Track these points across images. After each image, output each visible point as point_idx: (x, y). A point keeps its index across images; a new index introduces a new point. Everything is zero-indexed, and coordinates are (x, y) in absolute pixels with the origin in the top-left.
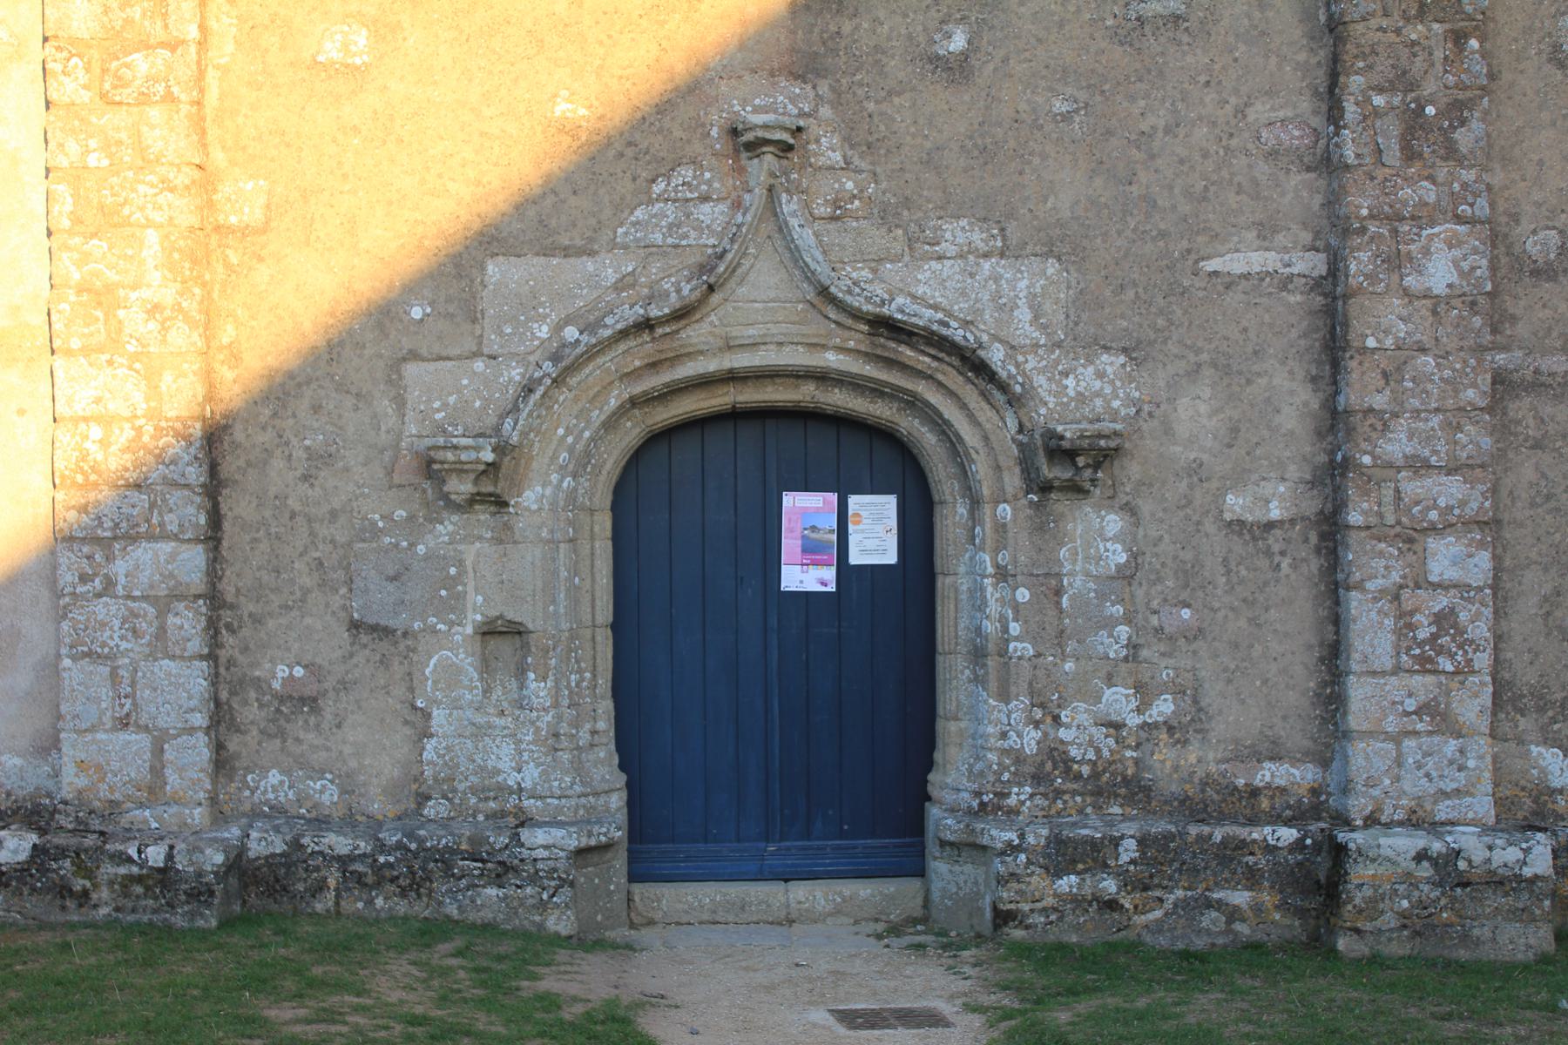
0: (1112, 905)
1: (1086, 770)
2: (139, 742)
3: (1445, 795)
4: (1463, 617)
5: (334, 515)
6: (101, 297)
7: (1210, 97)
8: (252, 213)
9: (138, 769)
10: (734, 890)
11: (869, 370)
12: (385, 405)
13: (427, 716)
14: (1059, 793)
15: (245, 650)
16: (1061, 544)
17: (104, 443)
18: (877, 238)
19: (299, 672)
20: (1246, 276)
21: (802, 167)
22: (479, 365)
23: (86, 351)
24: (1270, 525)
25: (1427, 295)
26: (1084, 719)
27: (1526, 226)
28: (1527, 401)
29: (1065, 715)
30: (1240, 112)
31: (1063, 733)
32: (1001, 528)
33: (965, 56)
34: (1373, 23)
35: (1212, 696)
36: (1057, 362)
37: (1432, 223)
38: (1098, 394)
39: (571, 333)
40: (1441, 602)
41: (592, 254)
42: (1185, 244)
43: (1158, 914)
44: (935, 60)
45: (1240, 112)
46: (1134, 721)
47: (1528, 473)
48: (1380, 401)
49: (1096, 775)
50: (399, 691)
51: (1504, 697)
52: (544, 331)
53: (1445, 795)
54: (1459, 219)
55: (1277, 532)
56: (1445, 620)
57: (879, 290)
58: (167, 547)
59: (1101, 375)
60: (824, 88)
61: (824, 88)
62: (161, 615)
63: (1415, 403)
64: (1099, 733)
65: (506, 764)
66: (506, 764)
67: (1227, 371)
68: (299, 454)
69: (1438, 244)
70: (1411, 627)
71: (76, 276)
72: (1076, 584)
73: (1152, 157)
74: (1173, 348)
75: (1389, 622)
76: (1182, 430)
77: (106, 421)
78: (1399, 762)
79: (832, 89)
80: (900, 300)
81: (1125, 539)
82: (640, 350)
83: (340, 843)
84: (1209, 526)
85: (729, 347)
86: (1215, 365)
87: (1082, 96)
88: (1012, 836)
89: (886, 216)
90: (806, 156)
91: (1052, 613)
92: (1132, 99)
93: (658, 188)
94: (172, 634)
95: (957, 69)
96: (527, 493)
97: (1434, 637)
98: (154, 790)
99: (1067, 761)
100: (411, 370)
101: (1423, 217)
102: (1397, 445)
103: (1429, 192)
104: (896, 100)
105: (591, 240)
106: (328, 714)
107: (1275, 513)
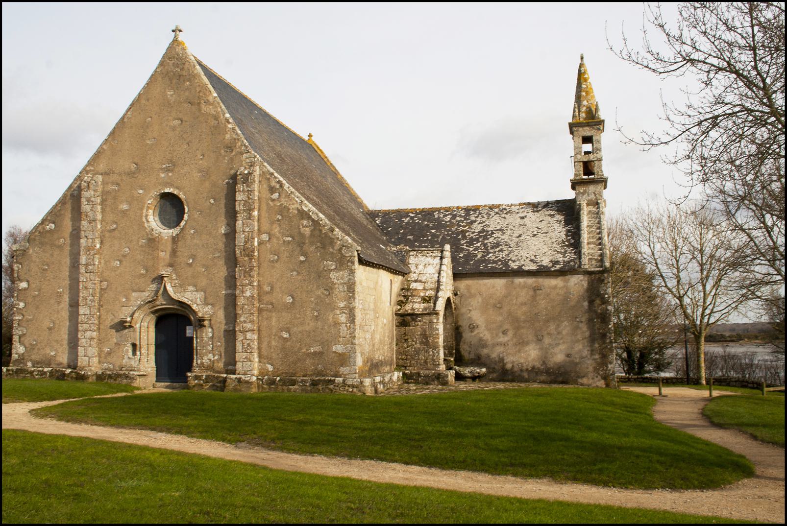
8: (105, 287)
11: (179, 308)
24: (230, 330)
28: (265, 312)
39: (142, 303)
46: (213, 359)
47: (265, 323)
48: (240, 312)
51: (260, 356)
56: (248, 344)
76: (219, 317)
77: (85, 315)
82: (151, 305)
83: (108, 373)
85: (162, 305)
89: (181, 286)
95: (190, 265)
100: (123, 308)
101: (246, 285)
102: (242, 319)
107: (231, 329)
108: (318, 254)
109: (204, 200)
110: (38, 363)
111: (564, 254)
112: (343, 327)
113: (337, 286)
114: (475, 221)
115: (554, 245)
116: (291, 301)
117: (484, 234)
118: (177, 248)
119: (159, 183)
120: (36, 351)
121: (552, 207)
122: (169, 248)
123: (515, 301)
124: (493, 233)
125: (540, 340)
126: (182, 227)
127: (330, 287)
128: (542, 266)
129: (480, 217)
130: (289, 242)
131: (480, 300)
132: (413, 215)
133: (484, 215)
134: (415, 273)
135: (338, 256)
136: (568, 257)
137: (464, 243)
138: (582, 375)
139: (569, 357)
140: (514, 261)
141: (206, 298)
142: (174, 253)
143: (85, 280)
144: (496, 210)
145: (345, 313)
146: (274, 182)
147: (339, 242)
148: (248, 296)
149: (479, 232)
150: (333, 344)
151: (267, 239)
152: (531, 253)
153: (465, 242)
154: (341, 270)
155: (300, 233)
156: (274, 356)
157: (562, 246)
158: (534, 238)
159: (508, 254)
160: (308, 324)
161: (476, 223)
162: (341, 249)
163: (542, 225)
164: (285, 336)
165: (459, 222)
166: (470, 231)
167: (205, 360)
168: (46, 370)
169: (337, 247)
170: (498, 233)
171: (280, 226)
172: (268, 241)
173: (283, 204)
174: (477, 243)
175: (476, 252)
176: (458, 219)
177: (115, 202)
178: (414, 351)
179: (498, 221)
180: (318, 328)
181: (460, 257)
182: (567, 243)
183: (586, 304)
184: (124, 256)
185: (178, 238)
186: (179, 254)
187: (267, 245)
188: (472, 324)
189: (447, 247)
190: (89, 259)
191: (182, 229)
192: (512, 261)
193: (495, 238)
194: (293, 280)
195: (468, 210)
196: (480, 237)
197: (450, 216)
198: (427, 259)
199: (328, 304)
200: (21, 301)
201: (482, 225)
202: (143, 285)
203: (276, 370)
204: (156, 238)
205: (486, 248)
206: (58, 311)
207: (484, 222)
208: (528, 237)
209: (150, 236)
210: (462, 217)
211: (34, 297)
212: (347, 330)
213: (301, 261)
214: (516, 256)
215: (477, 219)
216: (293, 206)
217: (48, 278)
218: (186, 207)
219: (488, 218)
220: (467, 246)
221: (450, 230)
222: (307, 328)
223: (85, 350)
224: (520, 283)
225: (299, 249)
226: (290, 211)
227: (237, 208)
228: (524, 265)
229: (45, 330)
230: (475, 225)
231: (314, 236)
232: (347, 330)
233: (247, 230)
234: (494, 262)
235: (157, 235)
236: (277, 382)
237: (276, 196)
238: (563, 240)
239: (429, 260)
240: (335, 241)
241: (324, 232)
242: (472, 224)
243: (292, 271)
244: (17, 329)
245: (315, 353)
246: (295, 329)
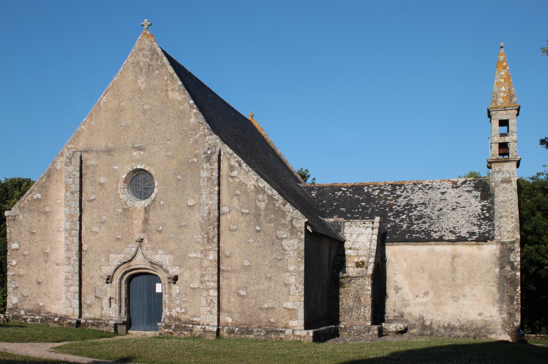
0: (171, 333)
1: (174, 318)
2: (72, 309)
3: (211, 322)
4: (214, 300)
5: (94, 284)
6: (69, 258)
7: (189, 235)
9: (72, 312)
10: (139, 331)
12: (99, 271)
13: (103, 308)
14: (171, 320)
15: (84, 299)
17: (69, 275)
18: (151, 252)
19: (90, 302)
20: (193, 257)
21: (143, 243)
22: (109, 267)
23: (67, 264)
24: (195, 288)
25: (210, 260)
26: (174, 311)
27: (226, 251)
28: (226, 273)
29: (172, 311)
30: (192, 237)
33: (161, 230)
34: (204, 226)
35: (188, 309)
37: (211, 251)
40: (211, 298)
41: (121, 254)
42: (185, 253)
43: (177, 334)
44: (158, 231)
45: (192, 237)
46: (180, 312)
49: (175, 318)
50: (100, 305)
52: (116, 263)
53: (211, 322)
54: (214, 251)
55: (196, 289)
56: (211, 300)
57: (152, 258)
58: (75, 287)
59: (176, 269)
60: (146, 234)
61: (146, 234)
62: (74, 295)
63: (208, 273)
65: (111, 314)
67: (190, 269)
68: (90, 277)
69: (211, 254)
70: (207, 301)
71: (67, 256)
72: (174, 295)
73: (182, 242)
74: (184, 266)
75: (205, 300)
76: (185, 276)
77: (69, 272)
78: (206, 318)
79: (147, 234)
81: (179, 289)
82: (125, 266)
83: (91, 321)
84: (188, 288)
86: (189, 268)
88: (161, 324)
92: (180, 235)
93: (128, 246)
94: (75, 297)
95: (160, 232)
97: (210, 302)
98: (73, 315)
99: (172, 316)
100: (102, 267)
101: (210, 250)
103: (210, 247)
106: (93, 307)
107: (196, 287)
108: (272, 224)
109: (172, 176)
110: (29, 312)
111: (479, 226)
112: (293, 287)
113: (288, 252)
114: (401, 196)
115: (471, 218)
116: (248, 264)
117: (409, 208)
118: (148, 217)
119: (132, 160)
120: (27, 301)
121: (469, 184)
122: (142, 215)
123: (435, 267)
124: (416, 207)
125: (456, 301)
126: (152, 199)
127: (282, 253)
128: (460, 236)
129: (405, 192)
130: (247, 214)
131: (405, 266)
132: (345, 189)
133: (409, 190)
134: (349, 241)
135: (289, 226)
136: (483, 229)
137: (391, 215)
138: (491, 331)
139: (481, 316)
140: (436, 232)
141: (175, 260)
142: (146, 221)
143: (69, 243)
144: (420, 186)
145: (293, 275)
146: (233, 161)
147: (290, 214)
148: (211, 259)
149: (404, 206)
150: (284, 301)
151: (228, 211)
152: (451, 225)
153: (391, 214)
154: (291, 239)
155: (256, 206)
156: (233, 310)
157: (478, 219)
158: (453, 212)
159: (430, 226)
160: (263, 284)
161: (402, 197)
162: (292, 220)
163: (460, 200)
164: (242, 294)
165: (386, 196)
166: (396, 205)
167: (174, 313)
168: (37, 317)
169: (289, 219)
170: (421, 207)
171: (239, 200)
172: (228, 212)
173: (241, 181)
174: (403, 215)
175: (402, 223)
176: (385, 193)
177: (93, 176)
178: (348, 309)
179: (421, 195)
180: (271, 287)
181: (388, 228)
182: (482, 217)
183: (497, 270)
184: (102, 223)
185: (149, 208)
186: (150, 222)
187: (228, 216)
188: (397, 286)
189: (377, 219)
190: (72, 225)
191: (154, 201)
192: (434, 231)
193: (419, 211)
194: (250, 247)
195: (394, 186)
196: (406, 210)
197: (378, 191)
198: (360, 229)
199: (280, 267)
200: (14, 259)
201: (407, 199)
202: (120, 248)
203: (235, 322)
204: (130, 207)
205: (411, 220)
206: (46, 268)
207: (409, 196)
208: (447, 211)
209: (125, 206)
210: (389, 191)
211: (25, 256)
212: (296, 290)
213: (257, 230)
214: (438, 227)
215: (402, 194)
216: (251, 183)
217: (36, 240)
218: (156, 182)
219: (412, 193)
220: (394, 218)
221: (378, 203)
222: (262, 287)
223: (70, 301)
224: (440, 251)
225: (255, 219)
226: (248, 187)
227: (202, 184)
228: (444, 235)
229: (35, 285)
230: (401, 199)
231: (269, 209)
232: (296, 290)
233: (210, 203)
234: (418, 232)
235: (131, 205)
236: (236, 332)
237: (235, 173)
238: (479, 214)
239: (362, 230)
240: (287, 213)
241: (277, 205)
242: (398, 198)
243: (249, 239)
244: (11, 283)
245: (268, 309)
246: (252, 288)
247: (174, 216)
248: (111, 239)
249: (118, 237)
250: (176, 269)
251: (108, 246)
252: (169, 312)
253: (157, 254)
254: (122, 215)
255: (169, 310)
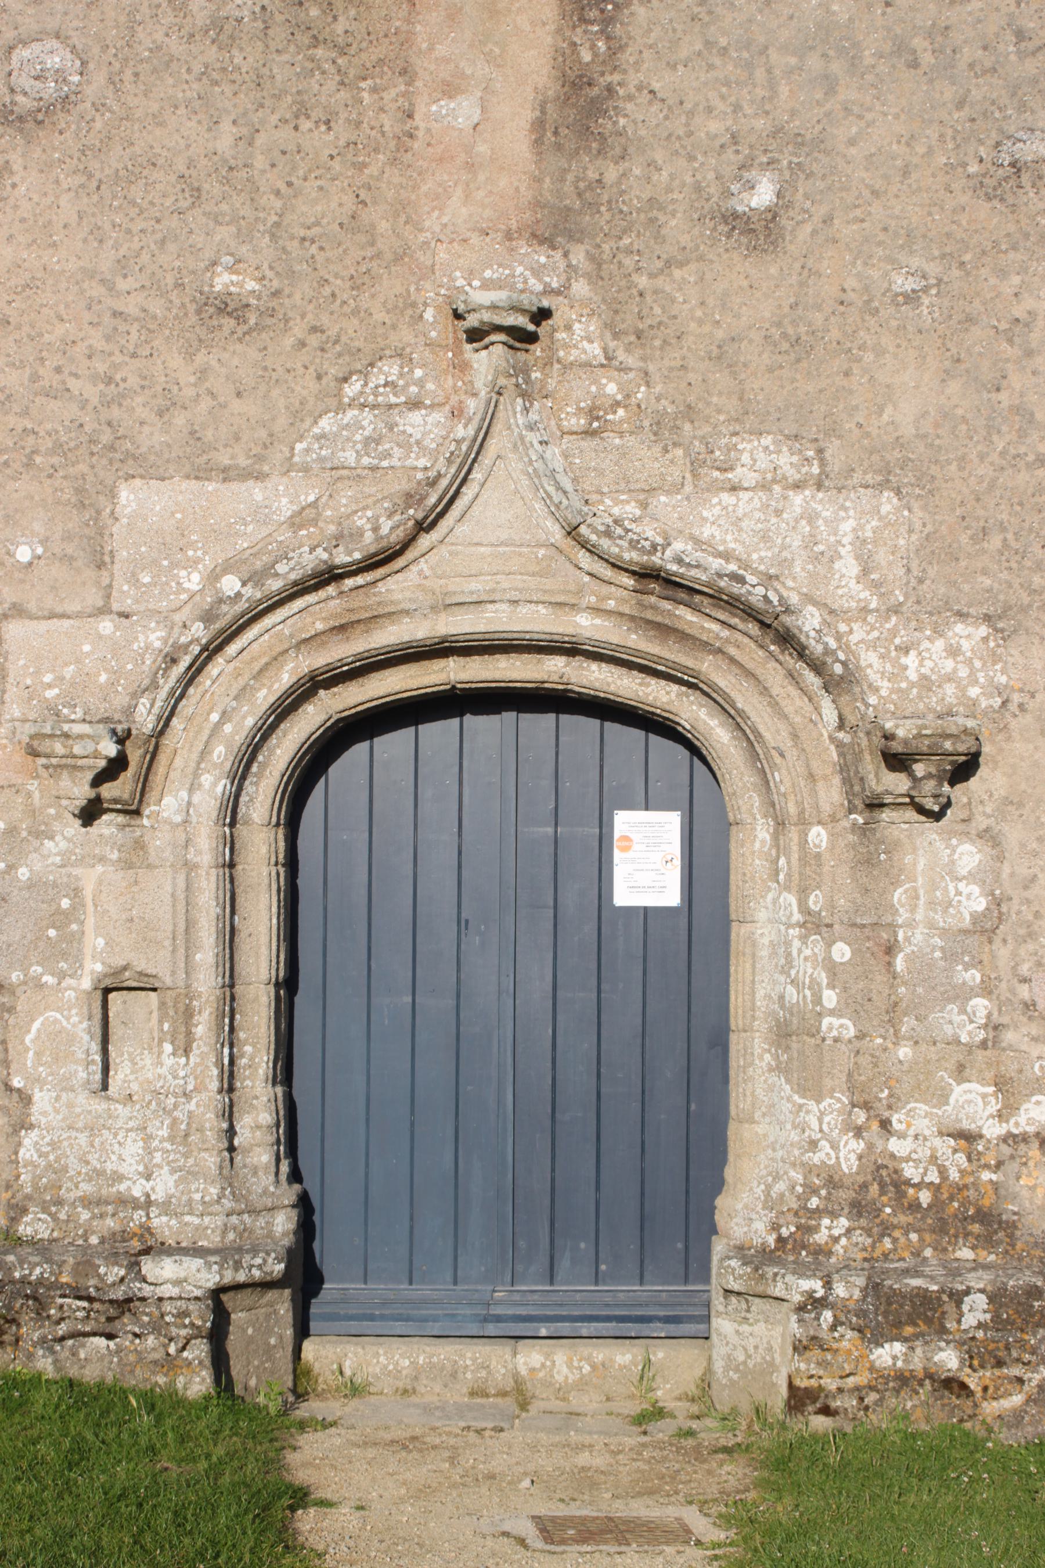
0: (953, 1385)
1: (925, 1197)
10: (444, 1352)
11: (636, 641)
13: (25, 1099)
14: (886, 1229)
16: (896, 884)
21: (548, 363)
22: (106, 626)
26: (923, 1125)
29: (897, 1121)
31: (895, 1145)
32: (810, 859)
33: (772, 214)
36: (894, 633)
38: (949, 678)
39: (230, 584)
41: (260, 477)
43: (1017, 1400)
46: (993, 1130)
49: (937, 1204)
52: (193, 581)
57: (650, 532)
59: (953, 652)
60: (579, 255)
61: (579, 255)
64: (944, 1146)
65: (131, 1167)
66: (131, 1167)
73: (1029, 353)
79: (591, 257)
80: (678, 546)
87: (933, 269)
88: (817, 1286)
90: (551, 349)
91: (880, 978)
92: (1003, 273)
93: (352, 389)
96: (167, 800)
99: (899, 1185)
104: (677, 273)
105: (260, 458)
247: (927, 59)
248: (131, 306)
249: (222, 280)
250: (953, 652)
251: (92, 392)
252: (858, 1132)
253: (716, 487)
254: (279, 34)
255: (860, 1117)
